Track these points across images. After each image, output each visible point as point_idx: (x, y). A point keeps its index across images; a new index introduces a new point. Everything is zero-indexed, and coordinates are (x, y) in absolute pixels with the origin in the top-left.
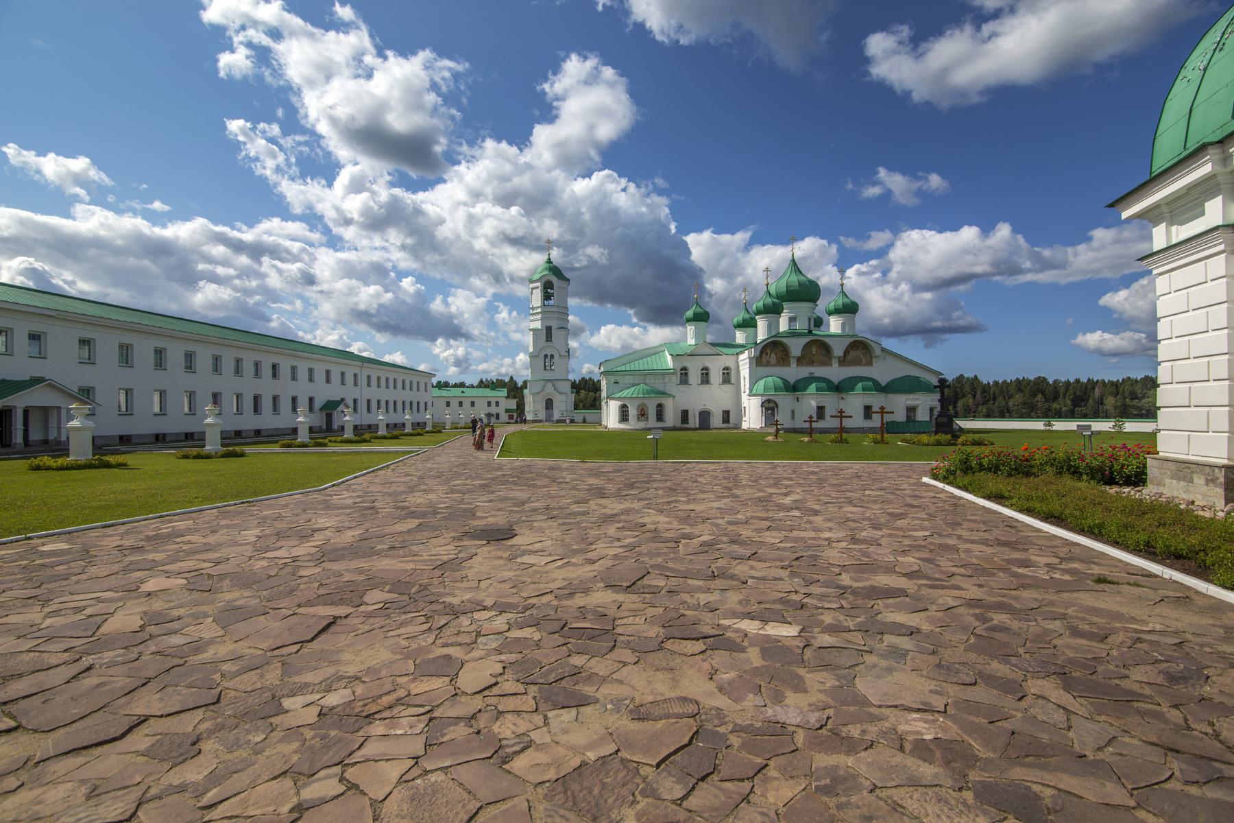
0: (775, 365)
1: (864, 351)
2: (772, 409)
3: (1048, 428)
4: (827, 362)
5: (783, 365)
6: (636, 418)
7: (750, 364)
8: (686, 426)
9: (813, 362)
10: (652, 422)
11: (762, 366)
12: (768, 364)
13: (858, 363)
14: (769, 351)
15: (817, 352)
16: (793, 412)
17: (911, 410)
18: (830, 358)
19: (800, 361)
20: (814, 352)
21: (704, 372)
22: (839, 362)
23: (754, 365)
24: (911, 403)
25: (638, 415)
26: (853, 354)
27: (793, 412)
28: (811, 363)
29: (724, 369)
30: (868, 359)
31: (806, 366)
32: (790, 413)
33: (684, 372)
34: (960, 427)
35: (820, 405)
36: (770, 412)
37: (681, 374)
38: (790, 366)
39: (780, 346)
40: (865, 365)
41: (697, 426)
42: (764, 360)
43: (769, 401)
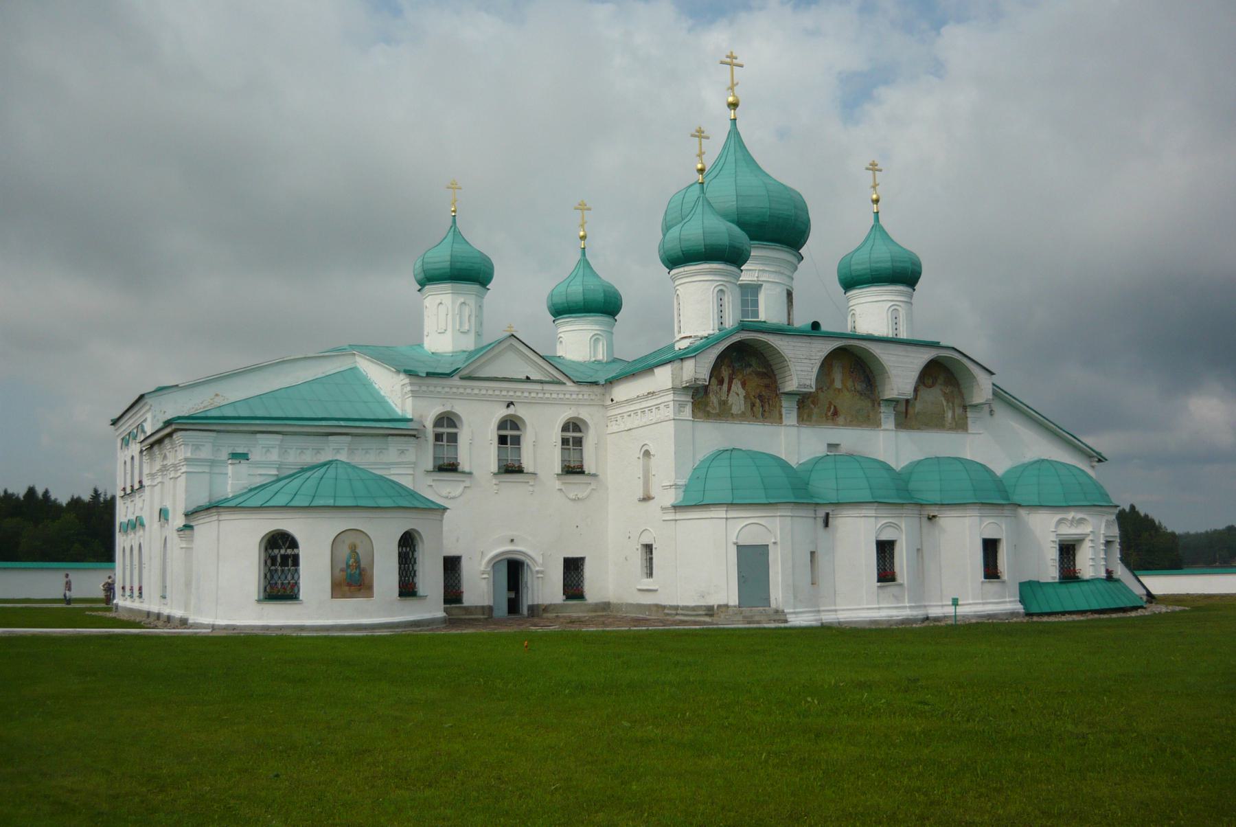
0: (742, 417)
4: (868, 420)
9: (835, 413)
11: (708, 416)
12: (724, 413)
13: (934, 422)
14: (725, 373)
15: (843, 382)
17: (1067, 550)
19: (806, 405)
20: (838, 384)
22: (897, 415)
24: (1070, 531)
26: (934, 396)
28: (833, 415)
29: (565, 428)
30: (959, 411)
34: (1149, 594)
35: (884, 537)
37: (438, 437)
39: (754, 362)
40: (951, 429)
42: (713, 399)
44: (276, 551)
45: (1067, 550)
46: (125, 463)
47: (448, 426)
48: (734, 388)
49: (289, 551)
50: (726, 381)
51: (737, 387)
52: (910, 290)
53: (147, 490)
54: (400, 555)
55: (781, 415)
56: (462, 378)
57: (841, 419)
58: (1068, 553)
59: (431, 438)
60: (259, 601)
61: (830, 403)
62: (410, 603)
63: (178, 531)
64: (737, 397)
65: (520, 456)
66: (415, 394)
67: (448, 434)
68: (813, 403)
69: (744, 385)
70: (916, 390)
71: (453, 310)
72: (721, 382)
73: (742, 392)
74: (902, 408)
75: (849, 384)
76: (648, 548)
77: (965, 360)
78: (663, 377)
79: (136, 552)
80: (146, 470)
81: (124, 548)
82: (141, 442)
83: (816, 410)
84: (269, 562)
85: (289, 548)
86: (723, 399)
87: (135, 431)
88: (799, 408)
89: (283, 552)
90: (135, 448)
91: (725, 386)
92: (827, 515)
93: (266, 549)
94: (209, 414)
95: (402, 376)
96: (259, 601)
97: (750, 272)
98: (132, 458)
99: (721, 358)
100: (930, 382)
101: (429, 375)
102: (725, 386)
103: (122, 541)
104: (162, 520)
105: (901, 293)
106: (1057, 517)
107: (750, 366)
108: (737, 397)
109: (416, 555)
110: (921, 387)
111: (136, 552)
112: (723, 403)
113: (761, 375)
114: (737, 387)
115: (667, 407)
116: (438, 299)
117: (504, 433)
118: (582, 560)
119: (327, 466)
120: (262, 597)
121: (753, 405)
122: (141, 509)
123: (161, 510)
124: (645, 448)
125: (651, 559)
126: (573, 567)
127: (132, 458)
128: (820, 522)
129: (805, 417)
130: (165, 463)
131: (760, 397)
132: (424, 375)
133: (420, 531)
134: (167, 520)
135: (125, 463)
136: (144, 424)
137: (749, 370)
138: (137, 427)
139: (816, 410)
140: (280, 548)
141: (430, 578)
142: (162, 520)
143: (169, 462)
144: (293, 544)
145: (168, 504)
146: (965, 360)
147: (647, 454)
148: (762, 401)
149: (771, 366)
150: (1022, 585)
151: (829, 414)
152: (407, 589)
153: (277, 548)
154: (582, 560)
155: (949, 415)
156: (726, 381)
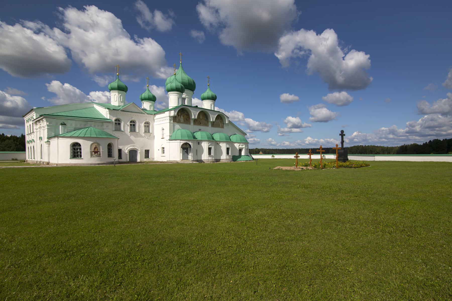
1: (221, 120)
2: (187, 149)
3: (273, 158)
5: (187, 123)
6: (90, 154)
7: (170, 120)
8: (120, 160)
9: (200, 123)
10: (104, 158)
14: (180, 114)
15: (202, 118)
16: (197, 150)
18: (208, 122)
20: (201, 118)
21: (132, 124)
23: (172, 122)
25: (91, 152)
26: (218, 121)
27: (197, 150)
28: (200, 124)
30: (222, 124)
31: (197, 125)
32: (196, 151)
33: (118, 122)
34: (253, 158)
35: (210, 147)
36: (185, 150)
37: (116, 124)
38: (190, 124)
39: (185, 112)
41: (128, 160)
43: (186, 144)
44: (75, 147)
45: (240, 150)
46: (28, 126)
47: (118, 121)
48: (181, 117)
49: (79, 147)
50: (180, 115)
51: (182, 117)
52: (214, 101)
53: (35, 133)
54: (108, 148)
55: (190, 123)
56: (121, 111)
57: (201, 125)
58: (240, 151)
59: (114, 124)
60: (70, 158)
61: (200, 121)
62: (110, 158)
63: (45, 142)
64: (182, 119)
65: (135, 128)
66: (110, 114)
67: (118, 123)
68: (196, 121)
69: (183, 116)
70: (215, 120)
71: (118, 97)
72: (179, 116)
73: (183, 118)
74: (213, 123)
75: (203, 118)
76: (163, 148)
77: (224, 115)
78: (167, 114)
79: (32, 148)
80: (35, 127)
81: (28, 147)
82: (33, 121)
83: (197, 123)
84: (73, 149)
85: (78, 146)
86: (179, 119)
87: (31, 118)
88: (194, 122)
89: (77, 147)
90: (31, 123)
91: (180, 117)
92: (199, 142)
93: (72, 146)
94: (53, 114)
95: (106, 109)
96: (70, 158)
97: (184, 95)
98: (30, 125)
99: (179, 111)
100: (218, 119)
101: (113, 109)
102: (180, 117)
103: (27, 145)
104: (40, 139)
105: (213, 102)
106: (239, 144)
107: (184, 113)
108: (182, 119)
109: (112, 148)
110: (216, 120)
111: (32, 148)
112: (179, 120)
113: (187, 115)
114: (182, 117)
115: (168, 120)
116: (114, 94)
117: (131, 123)
118: (149, 150)
119: (88, 128)
120: (71, 157)
121: (185, 121)
122: (34, 137)
123: (40, 137)
124: (163, 128)
125: (164, 150)
126: (147, 152)
127: (30, 125)
128: (198, 144)
129: (195, 124)
130: (40, 126)
131: (186, 119)
132: (112, 109)
133: (113, 143)
134: (42, 140)
135: (28, 126)
136: (33, 117)
137: (184, 114)
138: (31, 117)
139: (197, 123)
140: (76, 146)
141: (116, 154)
142: (40, 139)
143: (41, 126)
144: (81, 146)
145: (42, 136)
146: (224, 115)
147: (163, 129)
148: (187, 120)
149: (188, 113)
150: (232, 156)
151: (199, 123)
152: (110, 155)
153: (75, 146)
154: (149, 150)
155: (221, 125)
156: (180, 115)
